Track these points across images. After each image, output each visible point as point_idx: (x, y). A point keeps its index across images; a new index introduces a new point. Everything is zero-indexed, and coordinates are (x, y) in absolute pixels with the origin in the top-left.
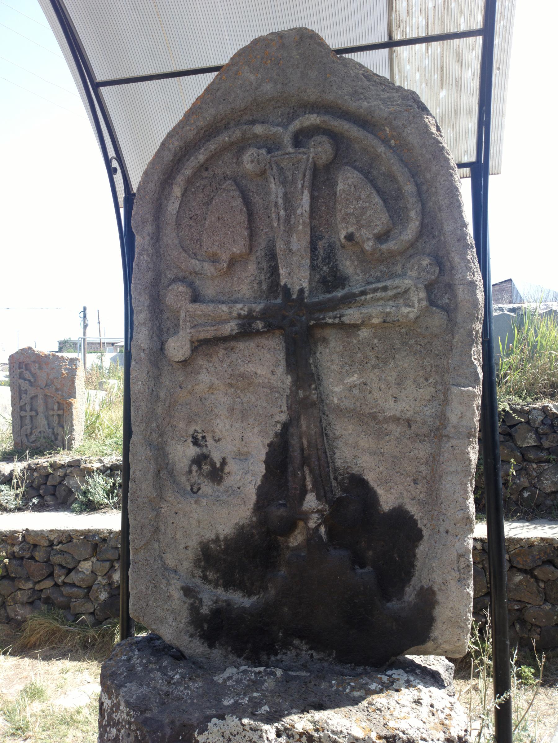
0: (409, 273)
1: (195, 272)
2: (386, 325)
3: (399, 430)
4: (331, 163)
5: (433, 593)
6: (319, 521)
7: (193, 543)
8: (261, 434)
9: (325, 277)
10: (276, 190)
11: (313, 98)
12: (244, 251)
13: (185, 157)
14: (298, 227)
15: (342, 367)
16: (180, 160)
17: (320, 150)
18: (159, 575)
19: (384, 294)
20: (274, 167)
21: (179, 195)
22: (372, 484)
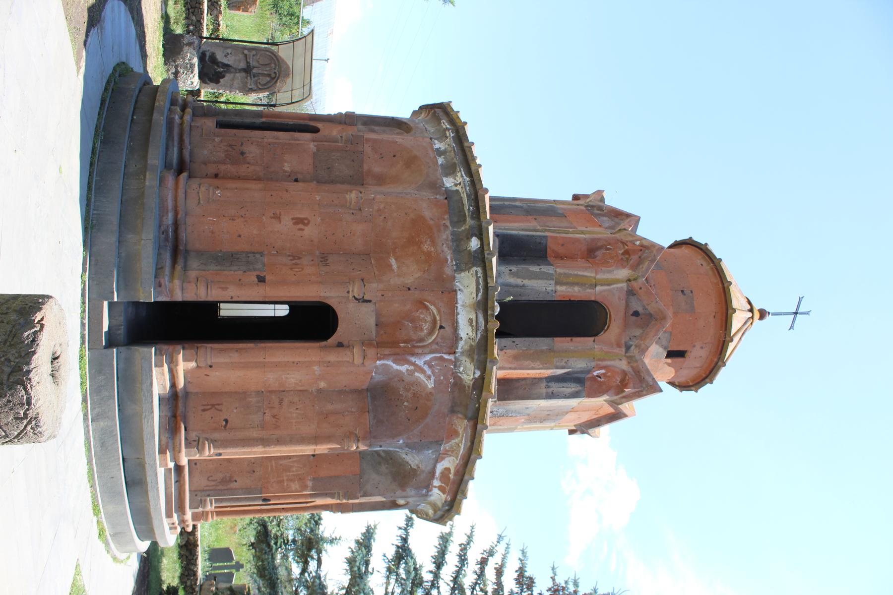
17: (273, 75)
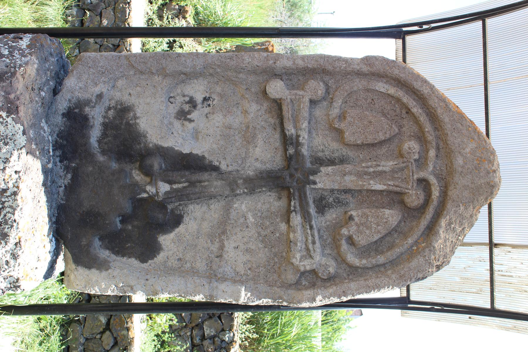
0: (324, 259)
1: (332, 102)
2: (289, 242)
3: (215, 249)
4: (405, 205)
5: (107, 270)
6: (150, 193)
7: (133, 100)
8: (211, 150)
9: (325, 199)
10: (387, 165)
11: (450, 193)
12: (346, 140)
13: (417, 96)
14: (361, 181)
15: (259, 211)
16: (415, 93)
17: (414, 198)
18: (111, 76)
19: (310, 241)
20: (404, 165)
21: (389, 92)
22: (177, 230)
